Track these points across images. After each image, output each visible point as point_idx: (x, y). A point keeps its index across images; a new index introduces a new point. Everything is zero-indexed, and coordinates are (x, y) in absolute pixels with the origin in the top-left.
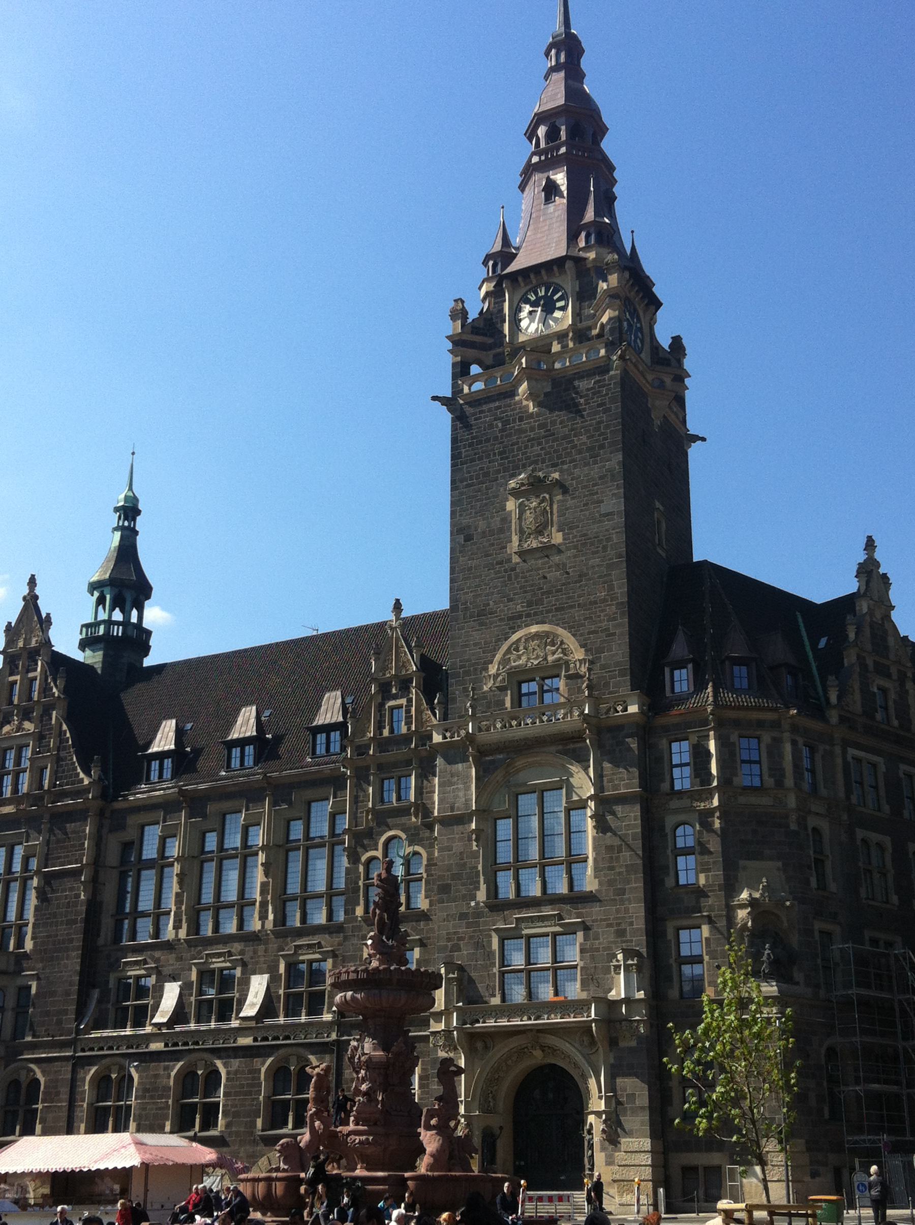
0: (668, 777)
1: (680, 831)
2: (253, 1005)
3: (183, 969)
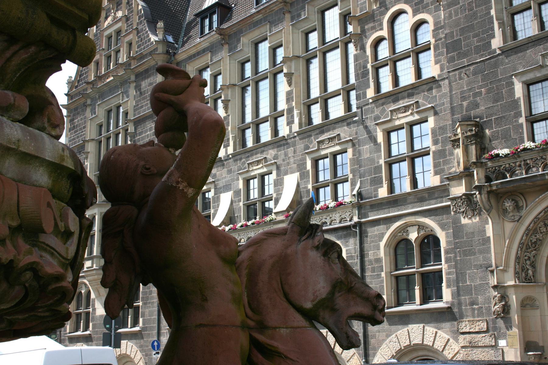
3: (233, 180)
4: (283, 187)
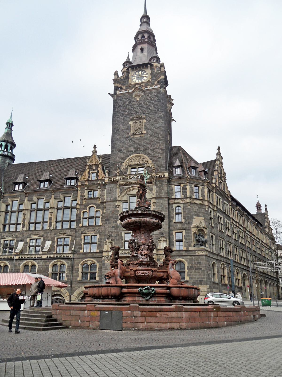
0: (174, 194)
1: (177, 208)
2: (46, 248)
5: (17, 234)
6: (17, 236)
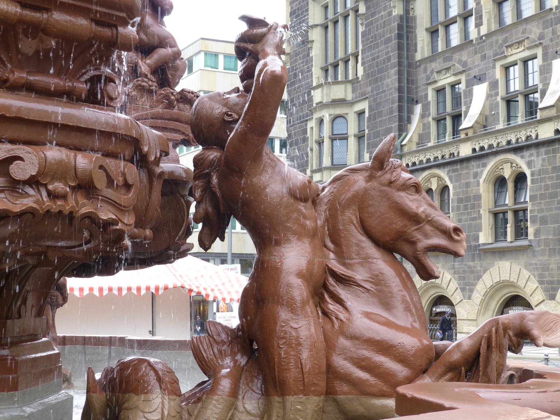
3: (488, 69)
4: (551, 75)
5: (464, 56)
6: (465, 64)
